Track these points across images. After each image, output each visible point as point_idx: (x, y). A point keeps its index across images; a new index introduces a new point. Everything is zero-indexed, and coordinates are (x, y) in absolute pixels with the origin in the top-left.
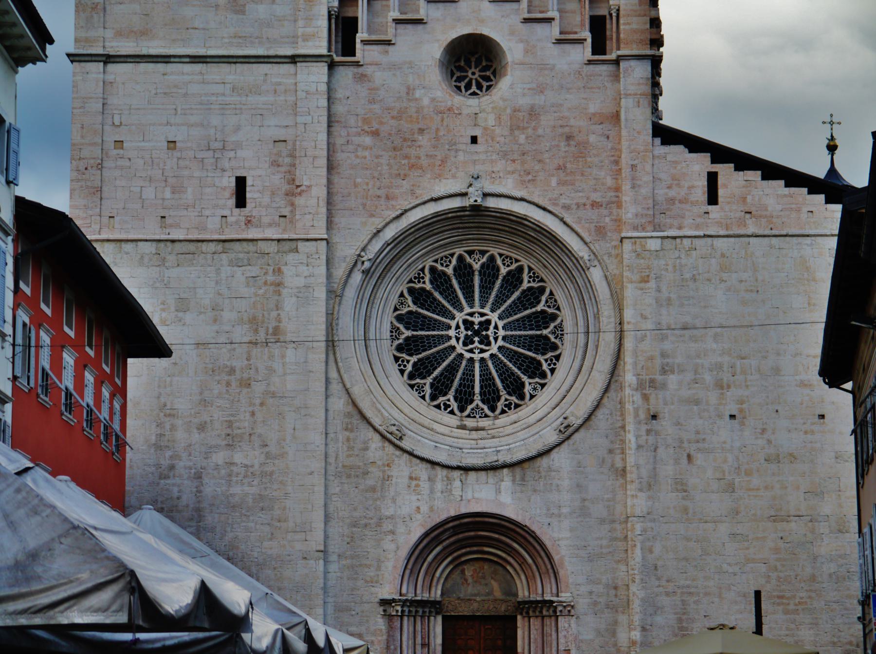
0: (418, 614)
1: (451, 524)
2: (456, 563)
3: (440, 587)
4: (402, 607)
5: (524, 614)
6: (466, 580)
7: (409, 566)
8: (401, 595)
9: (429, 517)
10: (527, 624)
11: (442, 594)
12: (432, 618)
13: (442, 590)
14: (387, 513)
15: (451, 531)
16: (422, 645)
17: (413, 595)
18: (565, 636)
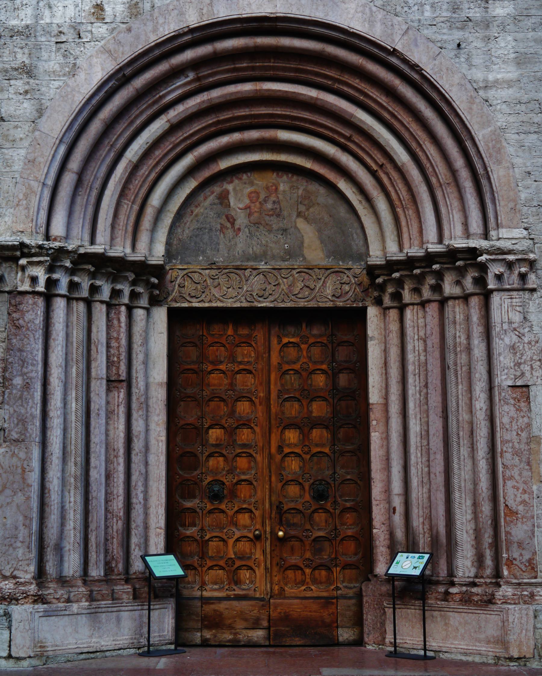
0: (97, 297)
1: (189, 55)
2: (206, 173)
3: (162, 235)
4: (51, 269)
5: (387, 301)
6: (232, 220)
7: (75, 164)
8: (47, 237)
9: (129, 30)
10: (394, 327)
11: (169, 254)
12: (139, 314)
13: (168, 244)
14: (14, 22)
15: (191, 76)
16: (109, 381)
17: (87, 243)
18: (513, 348)
